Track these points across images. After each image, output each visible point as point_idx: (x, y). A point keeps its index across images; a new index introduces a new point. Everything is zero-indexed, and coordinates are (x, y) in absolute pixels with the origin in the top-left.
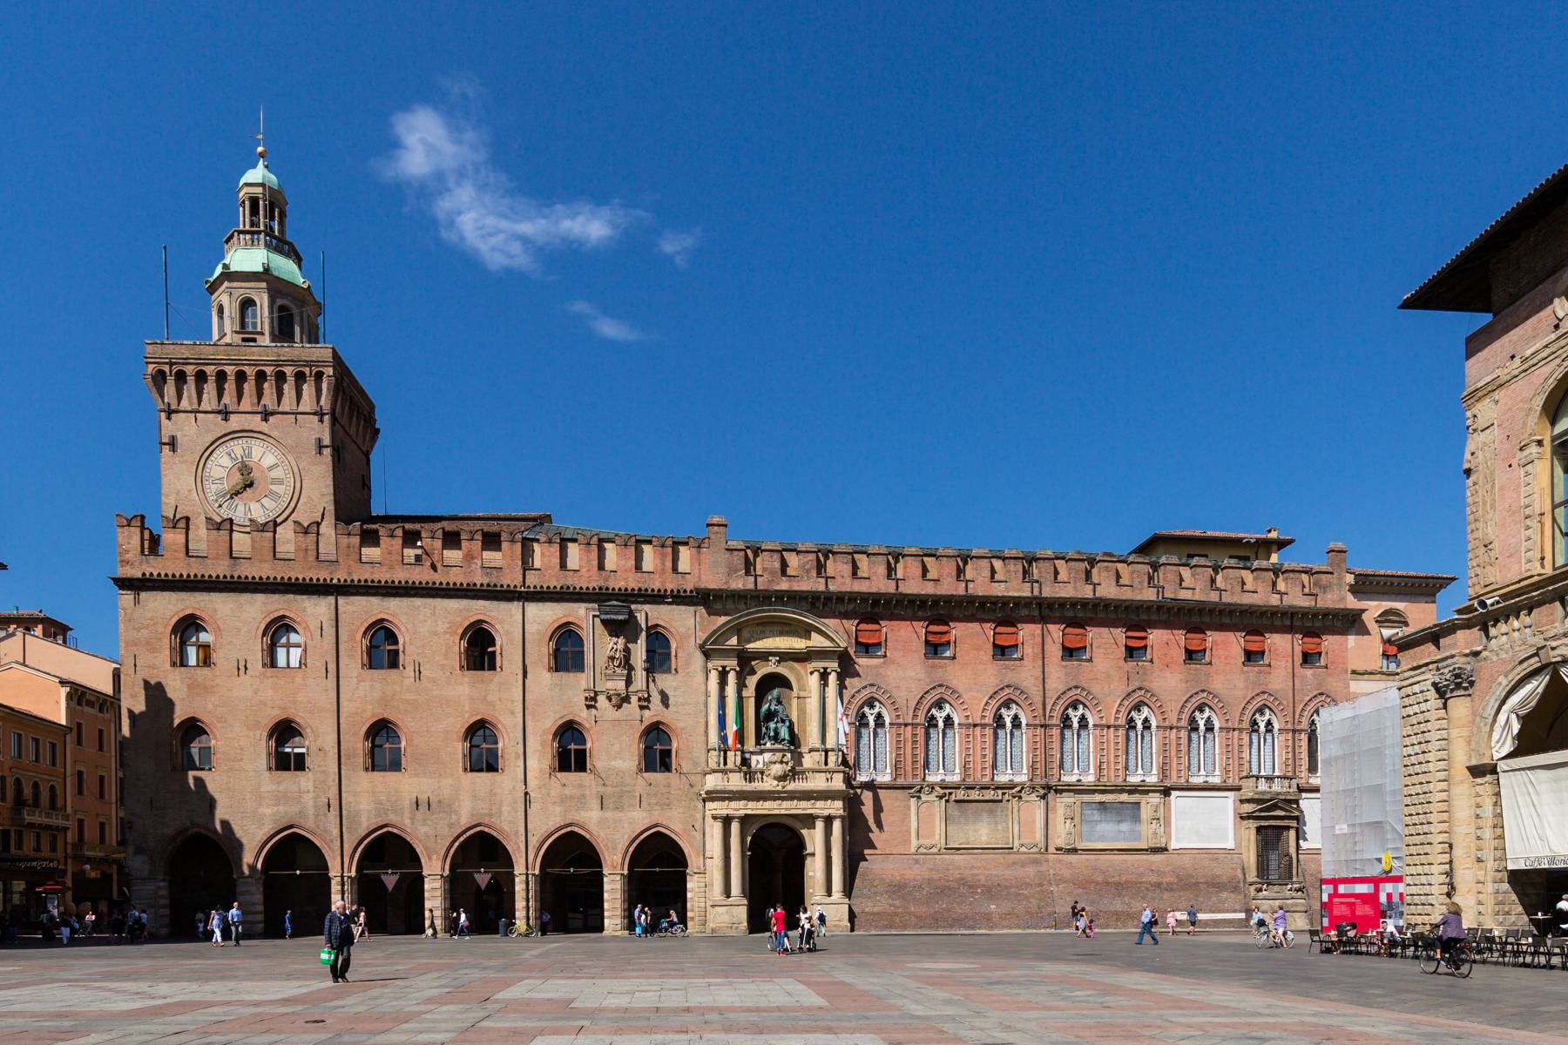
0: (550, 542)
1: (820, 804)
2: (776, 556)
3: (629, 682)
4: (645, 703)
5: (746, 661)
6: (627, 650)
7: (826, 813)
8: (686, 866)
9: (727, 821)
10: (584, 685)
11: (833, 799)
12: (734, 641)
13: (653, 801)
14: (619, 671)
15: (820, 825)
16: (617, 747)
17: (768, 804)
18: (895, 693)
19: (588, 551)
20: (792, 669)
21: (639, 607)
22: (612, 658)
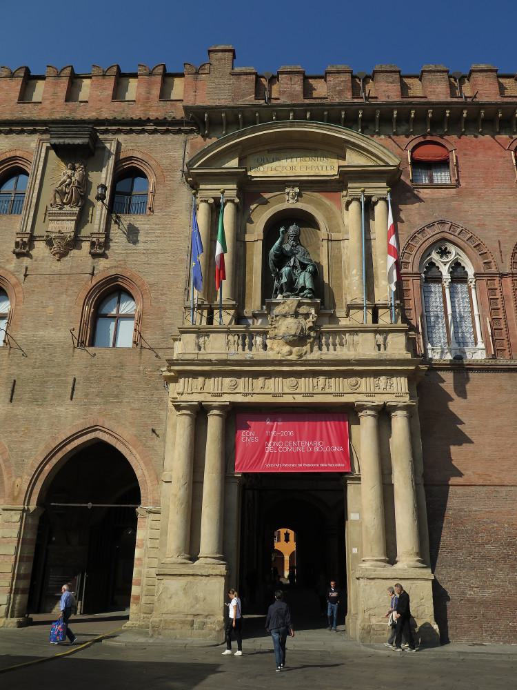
0: (12, 76)
1: (366, 384)
2: (298, 80)
3: (81, 220)
4: (100, 249)
5: (250, 192)
6: (85, 184)
7: (378, 400)
8: (136, 499)
9: (199, 413)
10: (18, 228)
11: (391, 374)
12: (234, 163)
13: (94, 390)
14: (67, 208)
15: (367, 424)
16: (50, 310)
17: (272, 385)
18: (478, 232)
19: (56, 84)
20: (319, 205)
21: (110, 136)
22: (62, 194)
